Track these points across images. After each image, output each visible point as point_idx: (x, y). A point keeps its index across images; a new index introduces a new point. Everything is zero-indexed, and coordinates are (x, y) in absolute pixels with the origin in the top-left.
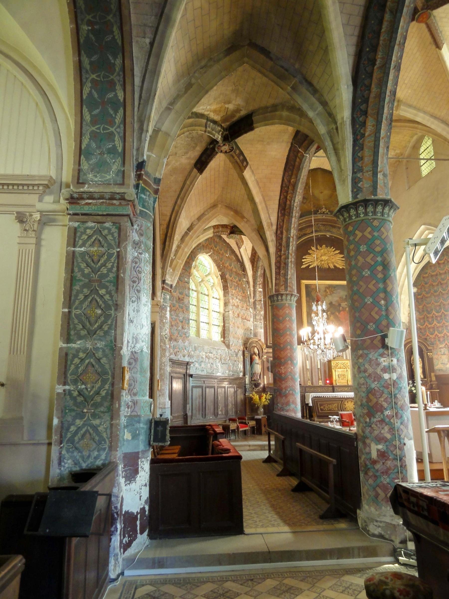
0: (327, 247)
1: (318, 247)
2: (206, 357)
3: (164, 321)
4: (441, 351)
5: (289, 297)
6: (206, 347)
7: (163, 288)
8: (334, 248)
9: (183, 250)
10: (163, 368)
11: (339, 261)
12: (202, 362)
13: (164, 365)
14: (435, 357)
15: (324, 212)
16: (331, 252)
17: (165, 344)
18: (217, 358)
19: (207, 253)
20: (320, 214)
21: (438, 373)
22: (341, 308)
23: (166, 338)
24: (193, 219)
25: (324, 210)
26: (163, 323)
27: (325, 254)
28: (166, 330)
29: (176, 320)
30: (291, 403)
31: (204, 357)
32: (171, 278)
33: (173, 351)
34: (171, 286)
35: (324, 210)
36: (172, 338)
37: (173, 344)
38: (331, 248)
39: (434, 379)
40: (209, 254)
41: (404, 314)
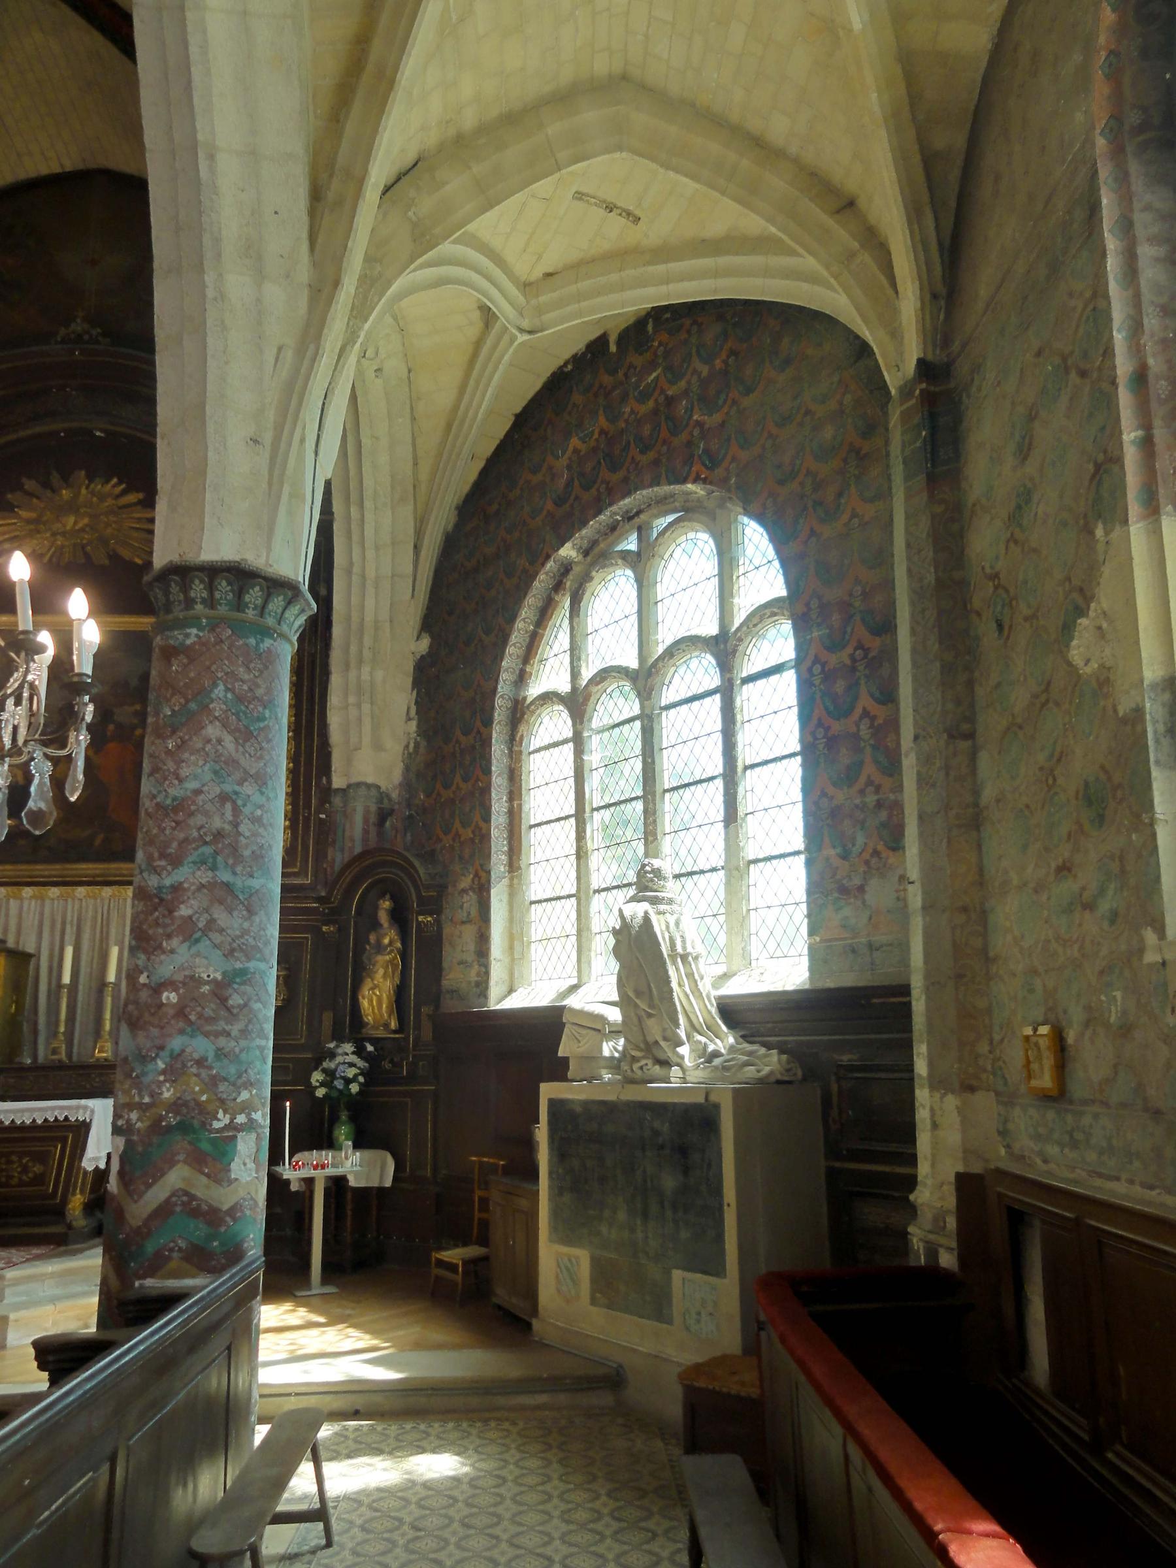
0: (91, 478)
1: (55, 478)
4: (462, 907)
8: (120, 482)
11: (135, 534)
14: (447, 930)
15: (80, 336)
16: (102, 498)
20: (63, 342)
21: (451, 1006)
22: (111, 727)
25: (78, 326)
27: (72, 507)
35: (78, 326)
38: (107, 482)
39: (427, 1033)
41: (378, 746)
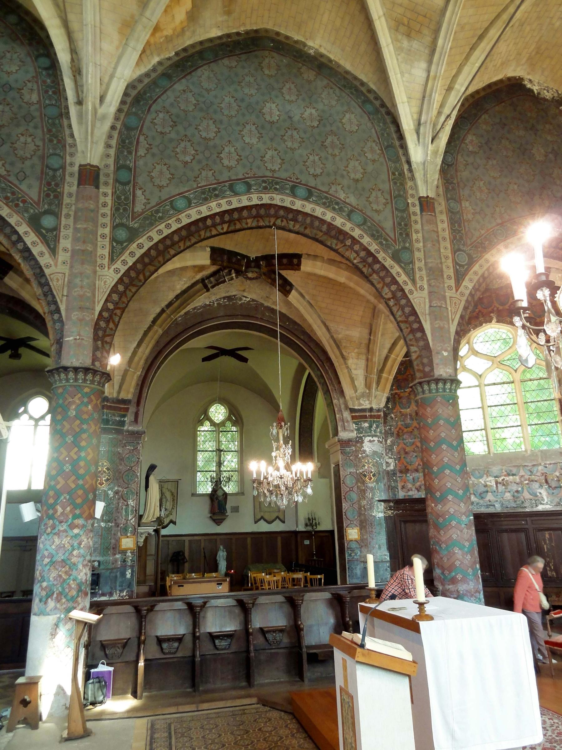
2: (497, 483)
3: (360, 456)
5: (420, 389)
6: (495, 470)
7: (353, 418)
9: (372, 360)
10: (363, 512)
12: (487, 492)
13: (365, 508)
17: (363, 482)
18: (532, 481)
19: (490, 321)
23: (365, 476)
24: (368, 321)
26: (359, 459)
28: (364, 466)
29: (413, 443)
30: (436, 566)
31: (493, 483)
32: (369, 400)
33: (413, 485)
34: (371, 410)
36: (408, 470)
37: (411, 477)
40: (494, 320)
